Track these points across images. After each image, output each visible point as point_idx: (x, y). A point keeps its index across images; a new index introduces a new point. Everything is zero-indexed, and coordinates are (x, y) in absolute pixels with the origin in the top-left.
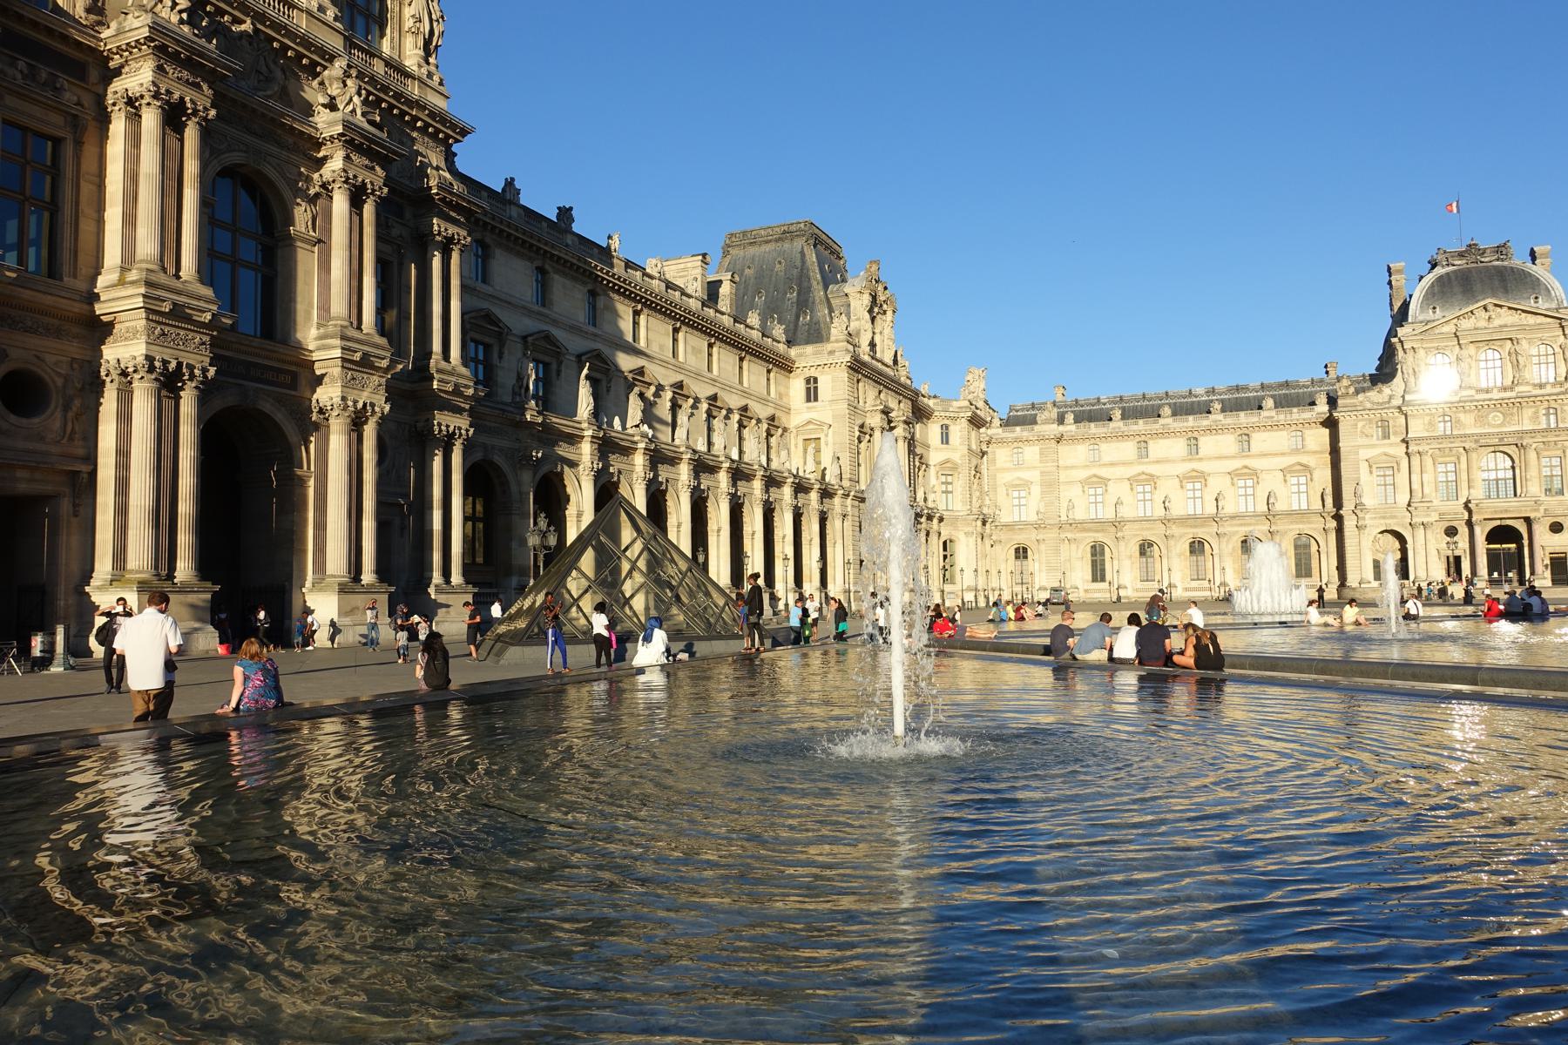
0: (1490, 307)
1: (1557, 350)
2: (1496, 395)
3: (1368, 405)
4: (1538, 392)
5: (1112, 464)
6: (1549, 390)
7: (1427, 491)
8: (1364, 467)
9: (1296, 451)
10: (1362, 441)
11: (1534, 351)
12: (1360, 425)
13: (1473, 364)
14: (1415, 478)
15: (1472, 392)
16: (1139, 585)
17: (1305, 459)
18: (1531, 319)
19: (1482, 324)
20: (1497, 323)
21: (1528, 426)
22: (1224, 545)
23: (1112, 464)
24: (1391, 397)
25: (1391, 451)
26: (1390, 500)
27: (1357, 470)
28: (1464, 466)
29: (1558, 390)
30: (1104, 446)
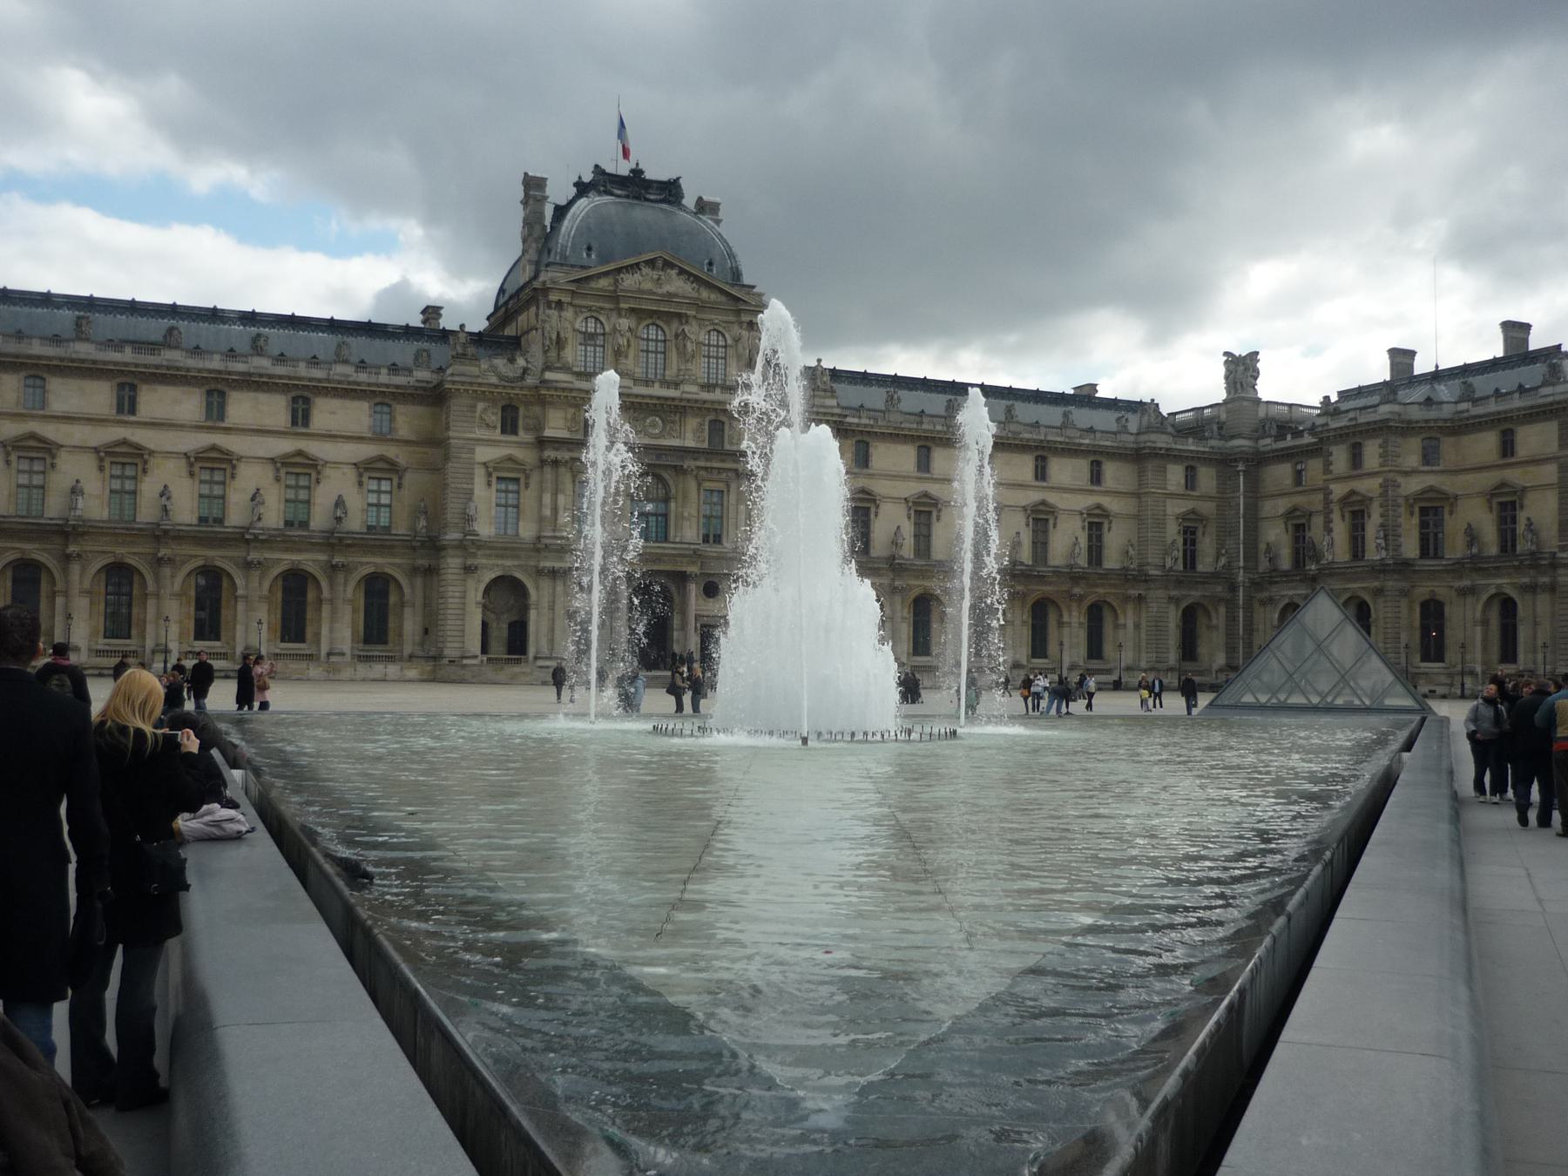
0: (660, 263)
2: (657, 390)
3: (494, 380)
4: (705, 396)
5: (68, 419)
8: (480, 474)
9: (379, 437)
10: (480, 433)
11: (703, 337)
14: (547, 498)
16: (102, 643)
17: (391, 451)
18: (705, 294)
19: (647, 285)
20: (667, 288)
21: (690, 443)
22: (255, 582)
23: (68, 419)
24: (525, 371)
25: (519, 454)
26: (510, 532)
30: (55, 384)
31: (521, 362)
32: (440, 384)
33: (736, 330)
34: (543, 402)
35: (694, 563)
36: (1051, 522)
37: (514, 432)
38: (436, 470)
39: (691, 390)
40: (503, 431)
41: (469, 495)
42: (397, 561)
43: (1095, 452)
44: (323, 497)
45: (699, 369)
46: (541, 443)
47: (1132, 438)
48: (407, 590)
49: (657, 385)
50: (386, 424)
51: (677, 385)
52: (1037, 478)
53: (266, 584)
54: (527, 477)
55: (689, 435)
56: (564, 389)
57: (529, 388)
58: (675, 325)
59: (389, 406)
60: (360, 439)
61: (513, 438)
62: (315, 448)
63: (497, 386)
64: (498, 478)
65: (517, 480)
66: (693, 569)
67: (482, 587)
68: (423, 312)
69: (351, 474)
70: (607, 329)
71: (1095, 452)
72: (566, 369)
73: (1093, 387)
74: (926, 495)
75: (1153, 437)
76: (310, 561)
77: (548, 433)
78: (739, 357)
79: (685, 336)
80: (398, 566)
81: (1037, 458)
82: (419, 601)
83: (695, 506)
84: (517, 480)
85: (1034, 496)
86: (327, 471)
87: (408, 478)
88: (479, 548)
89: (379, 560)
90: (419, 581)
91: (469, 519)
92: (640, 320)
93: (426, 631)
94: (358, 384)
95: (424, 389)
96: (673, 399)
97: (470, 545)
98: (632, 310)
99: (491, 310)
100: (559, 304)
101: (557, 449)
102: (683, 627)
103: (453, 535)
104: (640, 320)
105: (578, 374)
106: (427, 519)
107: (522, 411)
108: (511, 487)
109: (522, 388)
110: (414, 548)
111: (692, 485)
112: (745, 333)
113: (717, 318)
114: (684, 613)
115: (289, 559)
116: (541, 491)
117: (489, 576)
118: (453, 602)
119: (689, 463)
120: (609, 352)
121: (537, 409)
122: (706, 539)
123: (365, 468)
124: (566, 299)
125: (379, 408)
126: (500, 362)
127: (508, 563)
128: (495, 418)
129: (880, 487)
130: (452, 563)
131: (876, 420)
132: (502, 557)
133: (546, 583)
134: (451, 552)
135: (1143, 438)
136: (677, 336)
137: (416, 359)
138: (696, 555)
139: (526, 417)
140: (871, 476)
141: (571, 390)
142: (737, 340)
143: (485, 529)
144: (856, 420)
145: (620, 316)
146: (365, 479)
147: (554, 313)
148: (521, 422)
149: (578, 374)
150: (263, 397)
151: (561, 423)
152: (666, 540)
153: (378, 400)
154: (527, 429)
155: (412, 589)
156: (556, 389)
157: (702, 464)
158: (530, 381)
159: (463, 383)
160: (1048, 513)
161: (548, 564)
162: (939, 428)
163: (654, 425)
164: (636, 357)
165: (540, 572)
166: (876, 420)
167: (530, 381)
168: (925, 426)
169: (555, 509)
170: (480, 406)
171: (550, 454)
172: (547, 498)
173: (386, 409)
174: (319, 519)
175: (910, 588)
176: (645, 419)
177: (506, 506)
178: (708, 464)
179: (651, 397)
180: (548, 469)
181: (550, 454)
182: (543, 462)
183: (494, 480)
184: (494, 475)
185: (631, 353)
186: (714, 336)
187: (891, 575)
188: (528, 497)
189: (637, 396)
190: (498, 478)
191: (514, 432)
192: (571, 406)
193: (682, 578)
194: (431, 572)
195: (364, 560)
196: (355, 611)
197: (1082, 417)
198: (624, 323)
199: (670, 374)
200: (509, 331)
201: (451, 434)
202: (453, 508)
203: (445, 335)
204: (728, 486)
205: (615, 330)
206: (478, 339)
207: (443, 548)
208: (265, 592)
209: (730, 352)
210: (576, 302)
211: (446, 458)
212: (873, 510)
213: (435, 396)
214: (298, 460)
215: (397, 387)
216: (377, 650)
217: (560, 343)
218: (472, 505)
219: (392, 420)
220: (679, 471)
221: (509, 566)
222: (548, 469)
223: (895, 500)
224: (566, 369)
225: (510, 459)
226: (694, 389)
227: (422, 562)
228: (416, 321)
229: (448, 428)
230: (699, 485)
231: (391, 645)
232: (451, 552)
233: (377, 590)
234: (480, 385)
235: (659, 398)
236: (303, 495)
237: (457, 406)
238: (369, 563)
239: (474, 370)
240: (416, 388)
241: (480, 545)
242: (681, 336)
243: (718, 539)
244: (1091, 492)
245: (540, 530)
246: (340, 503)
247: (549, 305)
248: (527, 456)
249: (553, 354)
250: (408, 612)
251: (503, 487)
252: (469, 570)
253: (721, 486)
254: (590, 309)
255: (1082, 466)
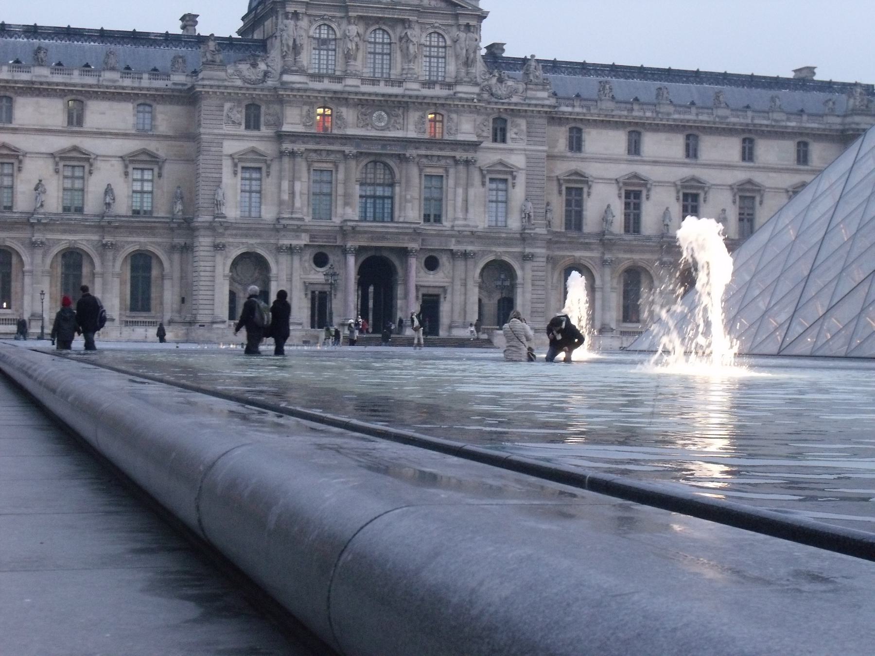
1: (449, 43)
2: (382, 88)
3: (239, 83)
4: (426, 92)
6: (437, 91)
7: (298, 204)
9: (141, 133)
12: (227, 106)
13: (361, 44)
15: (356, 82)
17: (152, 146)
21: (412, 134)
22: (38, 259)
24: (266, 74)
25: (261, 147)
26: (253, 214)
27: (219, 168)
28: (341, 176)
29: (445, 92)
31: (262, 66)
32: (193, 87)
33: (454, 32)
34: (281, 101)
35: (414, 240)
36: (758, 199)
37: (257, 127)
38: (191, 160)
39: (413, 88)
40: (247, 127)
41: (218, 182)
42: (159, 240)
43: (801, 134)
44: (95, 186)
45: (421, 69)
46: (280, 137)
47: (838, 120)
48: (166, 264)
49: (382, 83)
50: (147, 121)
51: (400, 83)
52: (744, 159)
53: (48, 261)
54: (268, 167)
55: (411, 127)
56: (299, 90)
57: (269, 90)
58: (399, 30)
59: (150, 106)
60: (126, 135)
61: (256, 133)
62: (88, 144)
63: (241, 88)
64: (243, 168)
65: (259, 169)
66: (413, 246)
67: (229, 262)
68: (183, 19)
69: (118, 166)
70: (339, 35)
71: (801, 134)
72: (302, 71)
73: (811, 70)
74: (636, 176)
75: (857, 119)
76: (85, 240)
77: (286, 128)
78: (457, 57)
79: (408, 40)
80: (159, 244)
81: (744, 140)
82: (177, 275)
83: (417, 189)
84: (259, 169)
85: (740, 176)
86: (99, 164)
87: (167, 168)
88: (226, 228)
89: (142, 239)
90: (176, 257)
91: (218, 204)
92: (367, 26)
93: (183, 300)
94: (123, 88)
95: (180, 91)
96: (396, 96)
97: (219, 226)
98: (361, 18)
99: (246, 11)
100: (296, 15)
101: (293, 142)
102: (406, 296)
103: (204, 218)
104: (367, 26)
105: (313, 76)
106: (183, 203)
107: (263, 109)
108: (255, 175)
109: (262, 90)
110: (172, 229)
111: (414, 171)
112: (462, 35)
113: (437, 22)
114: (406, 283)
115: (66, 239)
116: (280, 178)
117: (236, 252)
118: (204, 275)
119: (411, 152)
120: (340, 55)
121: (277, 107)
122: (427, 218)
123: (130, 161)
124: (301, 10)
125: (141, 108)
126: (244, 67)
127: (251, 241)
128: (240, 115)
129: (592, 170)
130: (204, 242)
131: (588, 108)
132: (246, 236)
133: (284, 259)
134: (202, 232)
135: (849, 120)
136: (401, 39)
137: (173, 65)
138: (417, 233)
139: (266, 114)
140: (583, 159)
141: (306, 90)
142: (455, 41)
143: (232, 212)
144: (569, 109)
145: (349, 23)
146: (130, 169)
147: (291, 23)
148: (262, 119)
149: (313, 76)
150: (44, 101)
151: (297, 119)
152: (392, 220)
153: (140, 101)
154: (268, 125)
155: (170, 264)
156: (292, 90)
157: (423, 152)
158: (270, 83)
159: (211, 86)
160: (753, 191)
161: (286, 242)
162: (649, 114)
163: (380, 119)
164: (365, 58)
165: (279, 249)
166: (588, 108)
167: (270, 83)
168: (635, 113)
169: (292, 194)
170: (227, 106)
171: (287, 146)
172: (285, 185)
173: (147, 109)
174: (92, 204)
175: (619, 261)
176: (372, 114)
177: (250, 192)
178: (429, 153)
179: (377, 95)
180: (286, 160)
181: (287, 146)
182: (281, 154)
183: (239, 169)
184: (240, 165)
185: (360, 56)
186: (434, 38)
187: (601, 249)
188: (269, 184)
189: (364, 94)
190: (243, 168)
191: (257, 127)
192: (305, 104)
193: (404, 253)
194: (187, 249)
195: (130, 239)
196: (122, 283)
197: (797, 98)
198: (353, 29)
199: (395, 73)
200: (257, 35)
201: (202, 130)
202: (204, 193)
203: (202, 40)
204: (447, 171)
205: (345, 36)
206: (226, 43)
207: (196, 229)
208: (47, 267)
209: (450, 51)
210: (310, 12)
211: (199, 152)
212: (585, 190)
213: (189, 98)
214: (74, 154)
215: (157, 90)
216: (141, 316)
217: (296, 49)
218: (220, 192)
219: (153, 118)
220: (402, 159)
221: (253, 244)
222: (286, 160)
223: (607, 181)
224: (302, 71)
225: (253, 151)
226: (415, 86)
227: (180, 241)
228: (176, 29)
229: (199, 125)
230: (421, 170)
231: (153, 313)
232: (202, 232)
233: (141, 265)
234: (226, 87)
235: (383, 95)
236: (78, 184)
237: (207, 106)
238: (134, 242)
239: (222, 74)
240: (173, 90)
241: (228, 226)
242: (405, 39)
243: (438, 219)
244: (797, 171)
245: (280, 213)
246: (109, 190)
247: (286, 15)
248: (267, 148)
249: (290, 59)
250: (167, 284)
251: (247, 175)
252: (218, 247)
253: (440, 172)
254: (322, 17)
255: (789, 147)
